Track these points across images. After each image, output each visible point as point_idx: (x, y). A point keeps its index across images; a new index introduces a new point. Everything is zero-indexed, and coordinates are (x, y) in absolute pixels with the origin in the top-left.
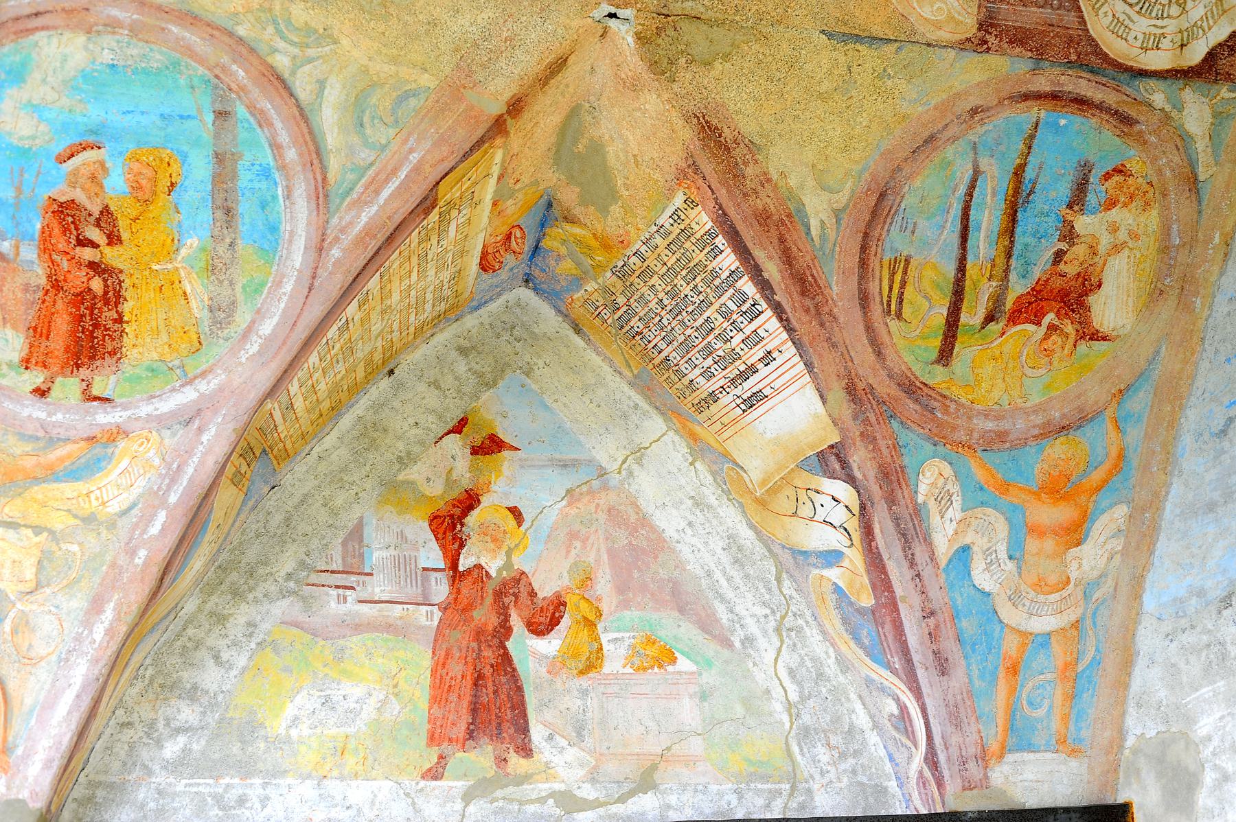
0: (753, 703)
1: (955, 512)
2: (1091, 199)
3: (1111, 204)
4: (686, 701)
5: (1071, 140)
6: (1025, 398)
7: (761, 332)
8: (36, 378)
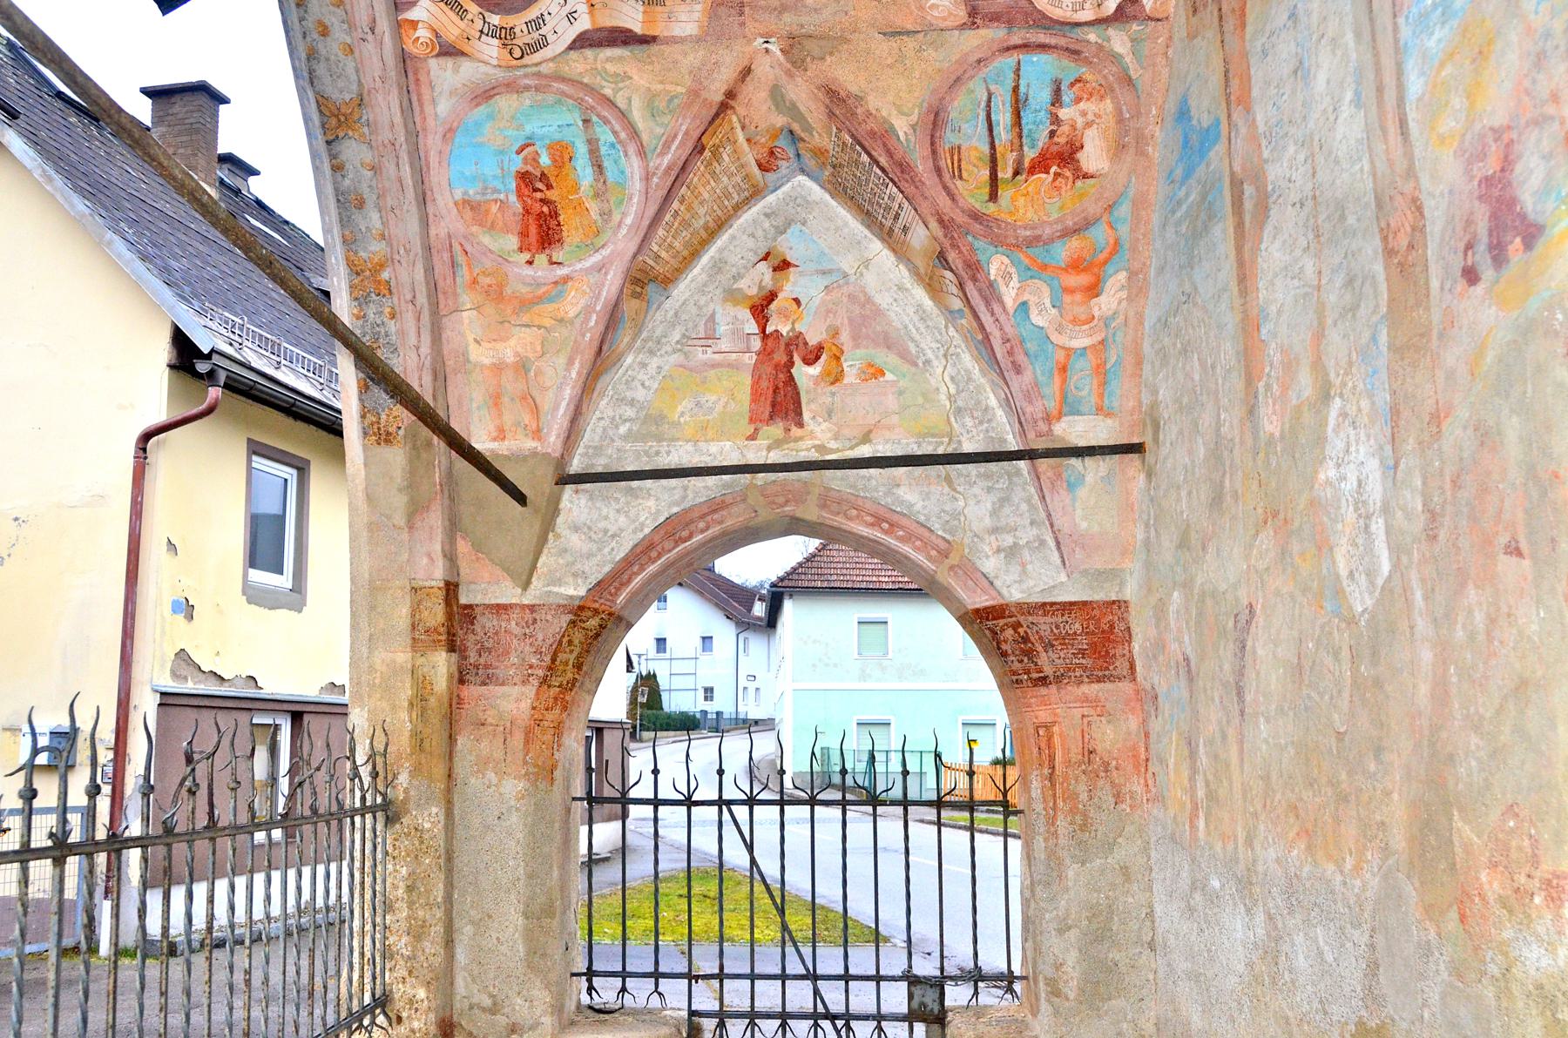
0: (929, 396)
1: (1015, 283)
2: (1066, 98)
3: (1078, 100)
4: (890, 396)
5: (1039, 71)
6: (1048, 215)
8: (527, 256)
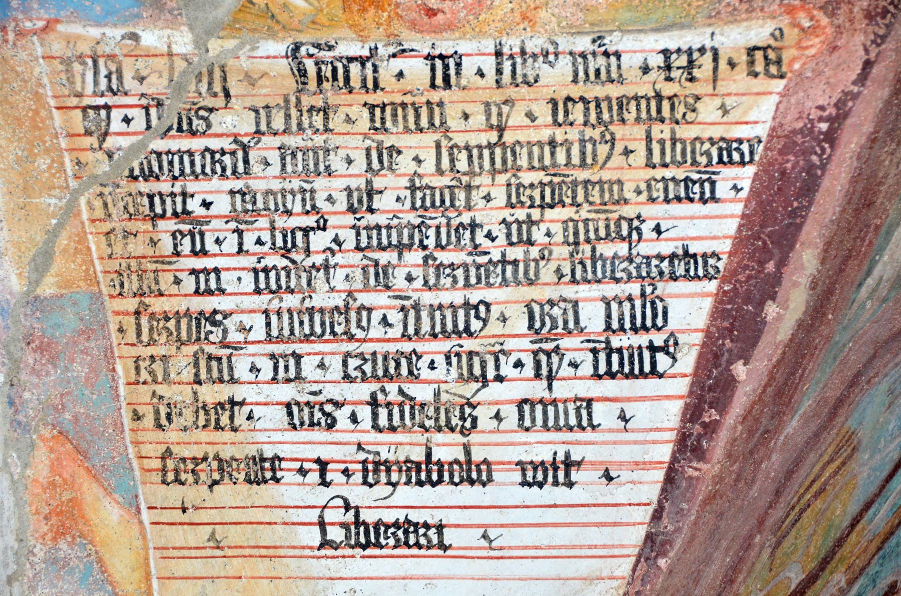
7: (603, 413)
